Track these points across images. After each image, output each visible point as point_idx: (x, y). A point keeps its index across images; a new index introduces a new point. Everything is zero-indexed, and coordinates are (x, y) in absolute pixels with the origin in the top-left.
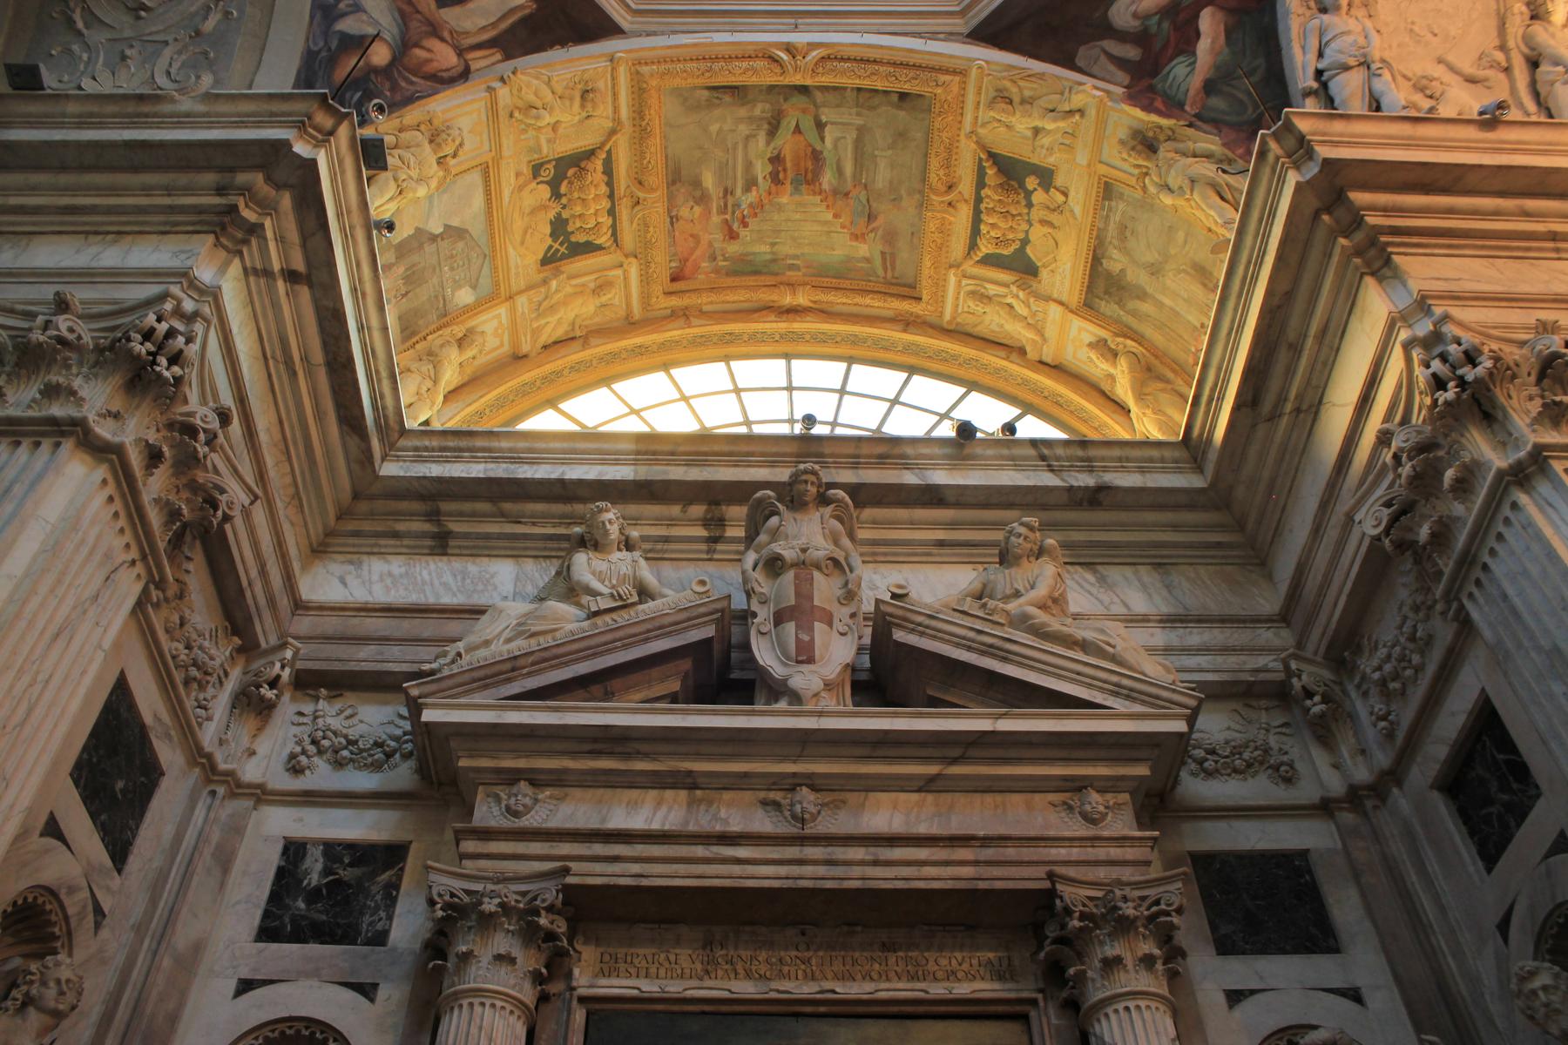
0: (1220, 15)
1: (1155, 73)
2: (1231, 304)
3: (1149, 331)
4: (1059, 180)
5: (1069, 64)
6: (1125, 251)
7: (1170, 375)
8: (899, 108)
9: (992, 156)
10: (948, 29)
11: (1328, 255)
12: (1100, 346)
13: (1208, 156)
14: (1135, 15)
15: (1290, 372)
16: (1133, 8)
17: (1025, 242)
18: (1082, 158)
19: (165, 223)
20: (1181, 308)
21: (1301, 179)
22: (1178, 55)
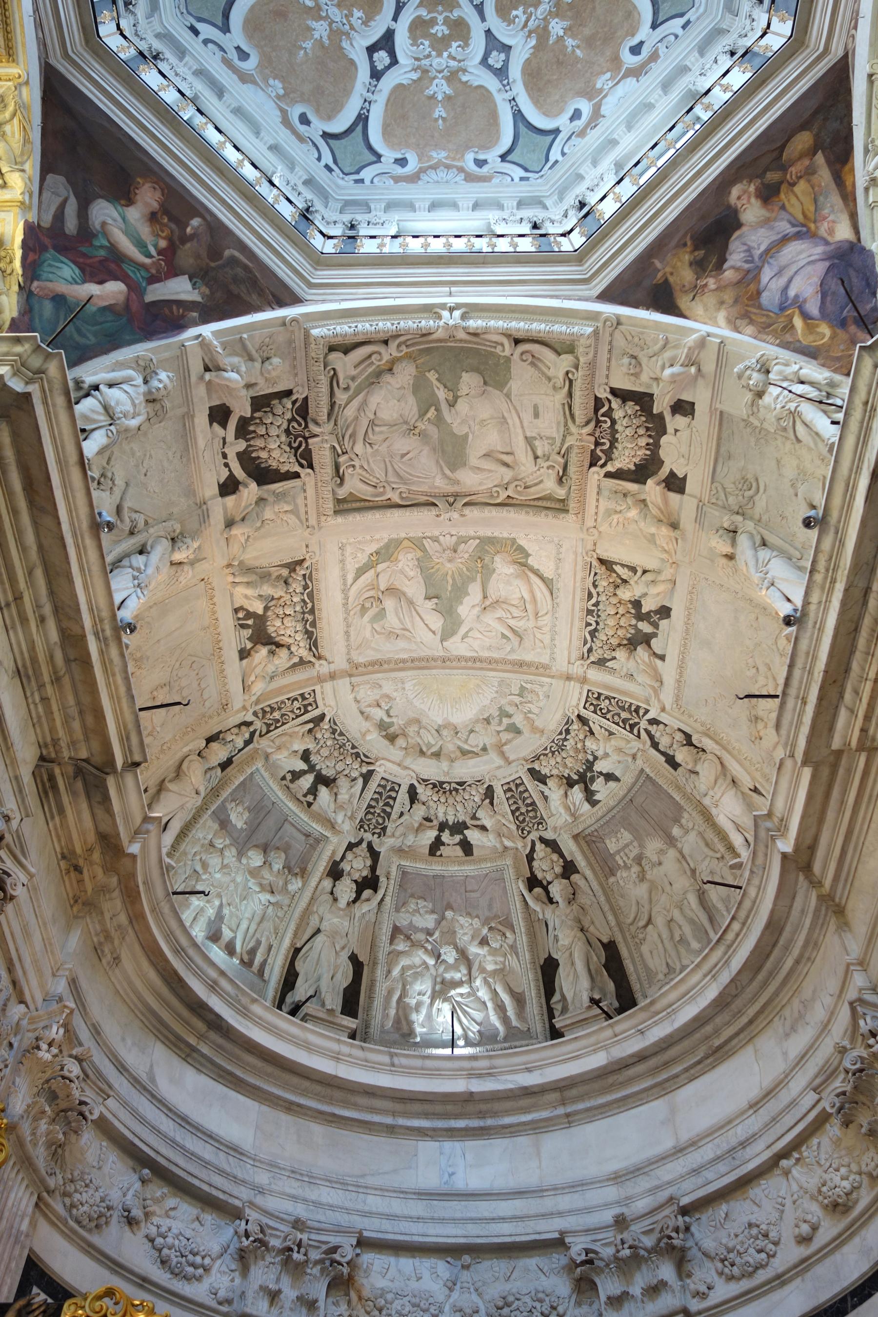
0: (121, 298)
5: (47, 168)
10: (48, 41)
14: (104, 224)
16: (110, 221)
21: (6, 379)
22: (82, 270)
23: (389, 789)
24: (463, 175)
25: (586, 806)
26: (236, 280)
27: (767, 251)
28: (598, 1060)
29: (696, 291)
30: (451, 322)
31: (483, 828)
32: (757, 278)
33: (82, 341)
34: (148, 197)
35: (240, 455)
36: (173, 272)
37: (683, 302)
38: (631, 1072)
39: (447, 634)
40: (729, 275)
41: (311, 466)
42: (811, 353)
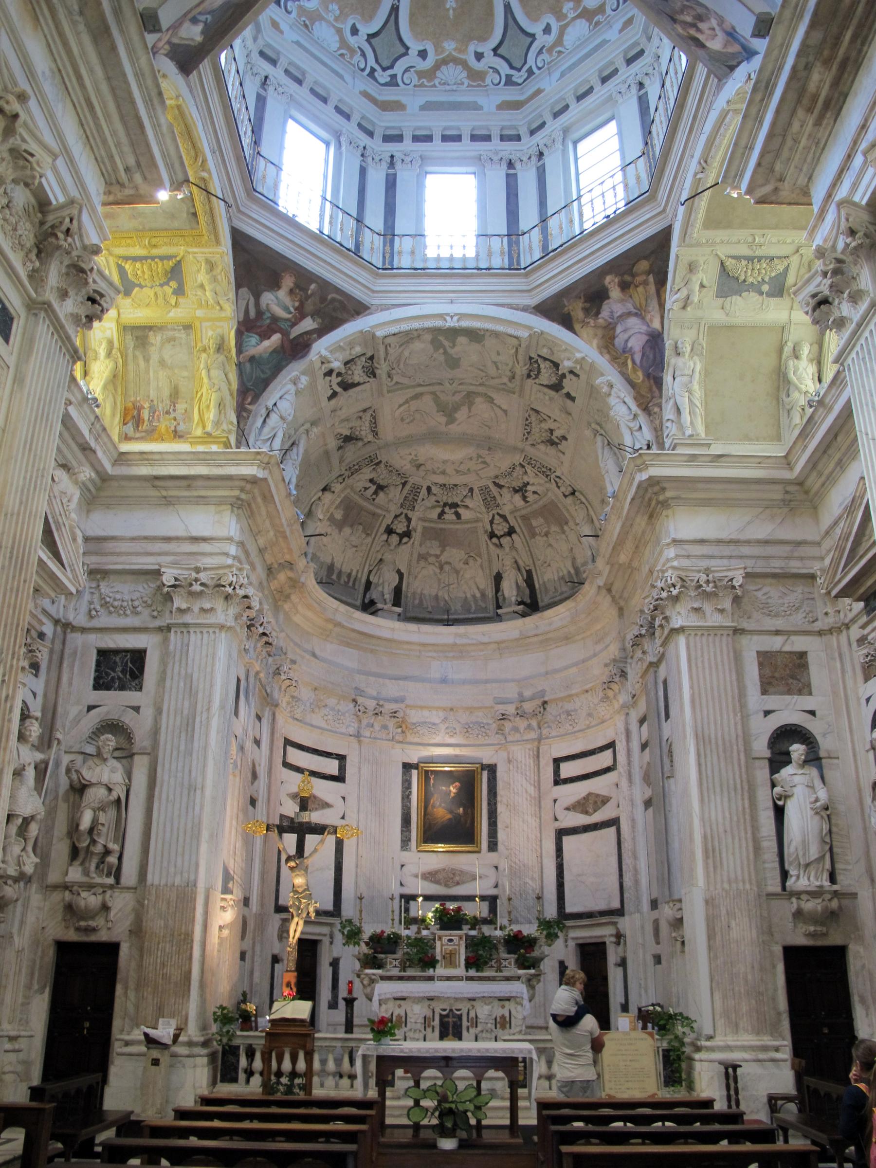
1: (248, 330)
2: (192, 456)
3: (131, 367)
4: (181, 300)
5: (238, 286)
6: (163, 344)
7: (119, 390)
8: (188, 213)
9: (179, 262)
11: (231, 488)
12: (110, 343)
13: (229, 384)
15: (179, 488)
17: (141, 287)
18: (199, 313)
19: (102, 157)
20: (153, 384)
22: (260, 336)
23: (416, 489)
24: (464, 74)
25: (522, 503)
26: (334, 310)
27: (620, 316)
28: (516, 634)
29: (584, 324)
30: (452, 325)
31: (467, 507)
32: (614, 329)
33: (263, 376)
34: (288, 282)
35: (339, 384)
36: (302, 317)
37: (577, 327)
38: (531, 640)
39: (447, 424)
40: (601, 321)
41: (375, 376)
42: (632, 384)
